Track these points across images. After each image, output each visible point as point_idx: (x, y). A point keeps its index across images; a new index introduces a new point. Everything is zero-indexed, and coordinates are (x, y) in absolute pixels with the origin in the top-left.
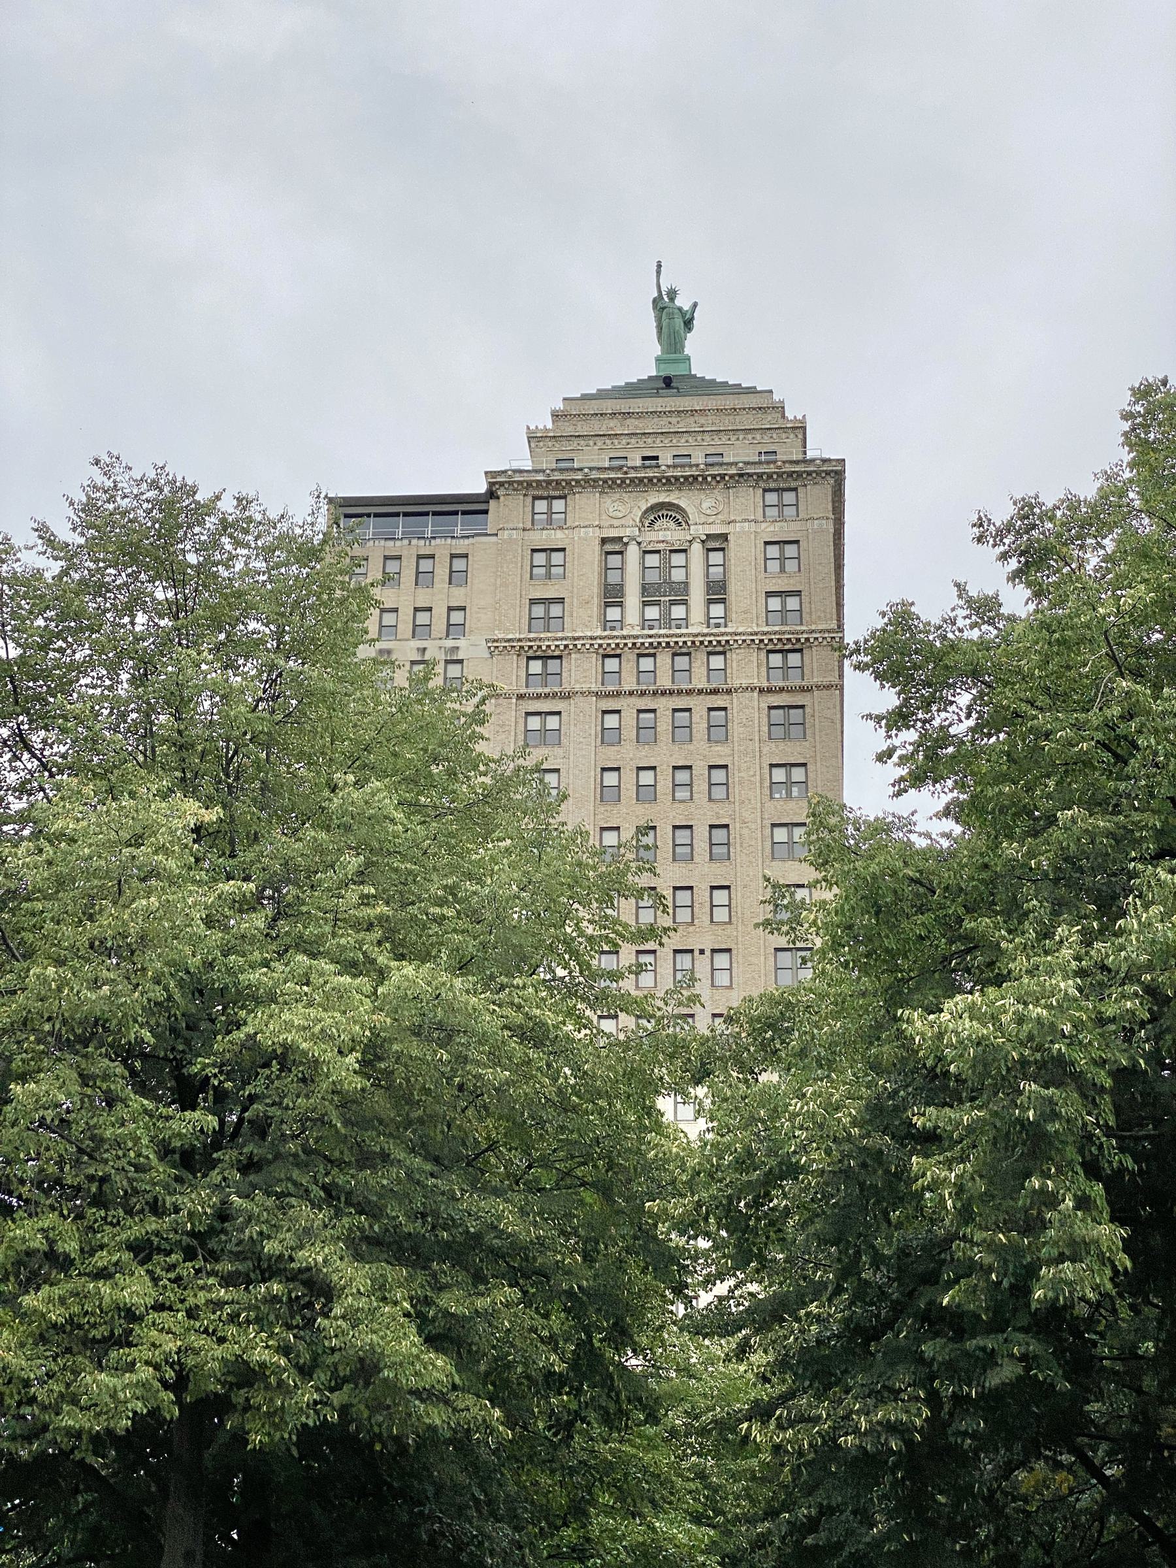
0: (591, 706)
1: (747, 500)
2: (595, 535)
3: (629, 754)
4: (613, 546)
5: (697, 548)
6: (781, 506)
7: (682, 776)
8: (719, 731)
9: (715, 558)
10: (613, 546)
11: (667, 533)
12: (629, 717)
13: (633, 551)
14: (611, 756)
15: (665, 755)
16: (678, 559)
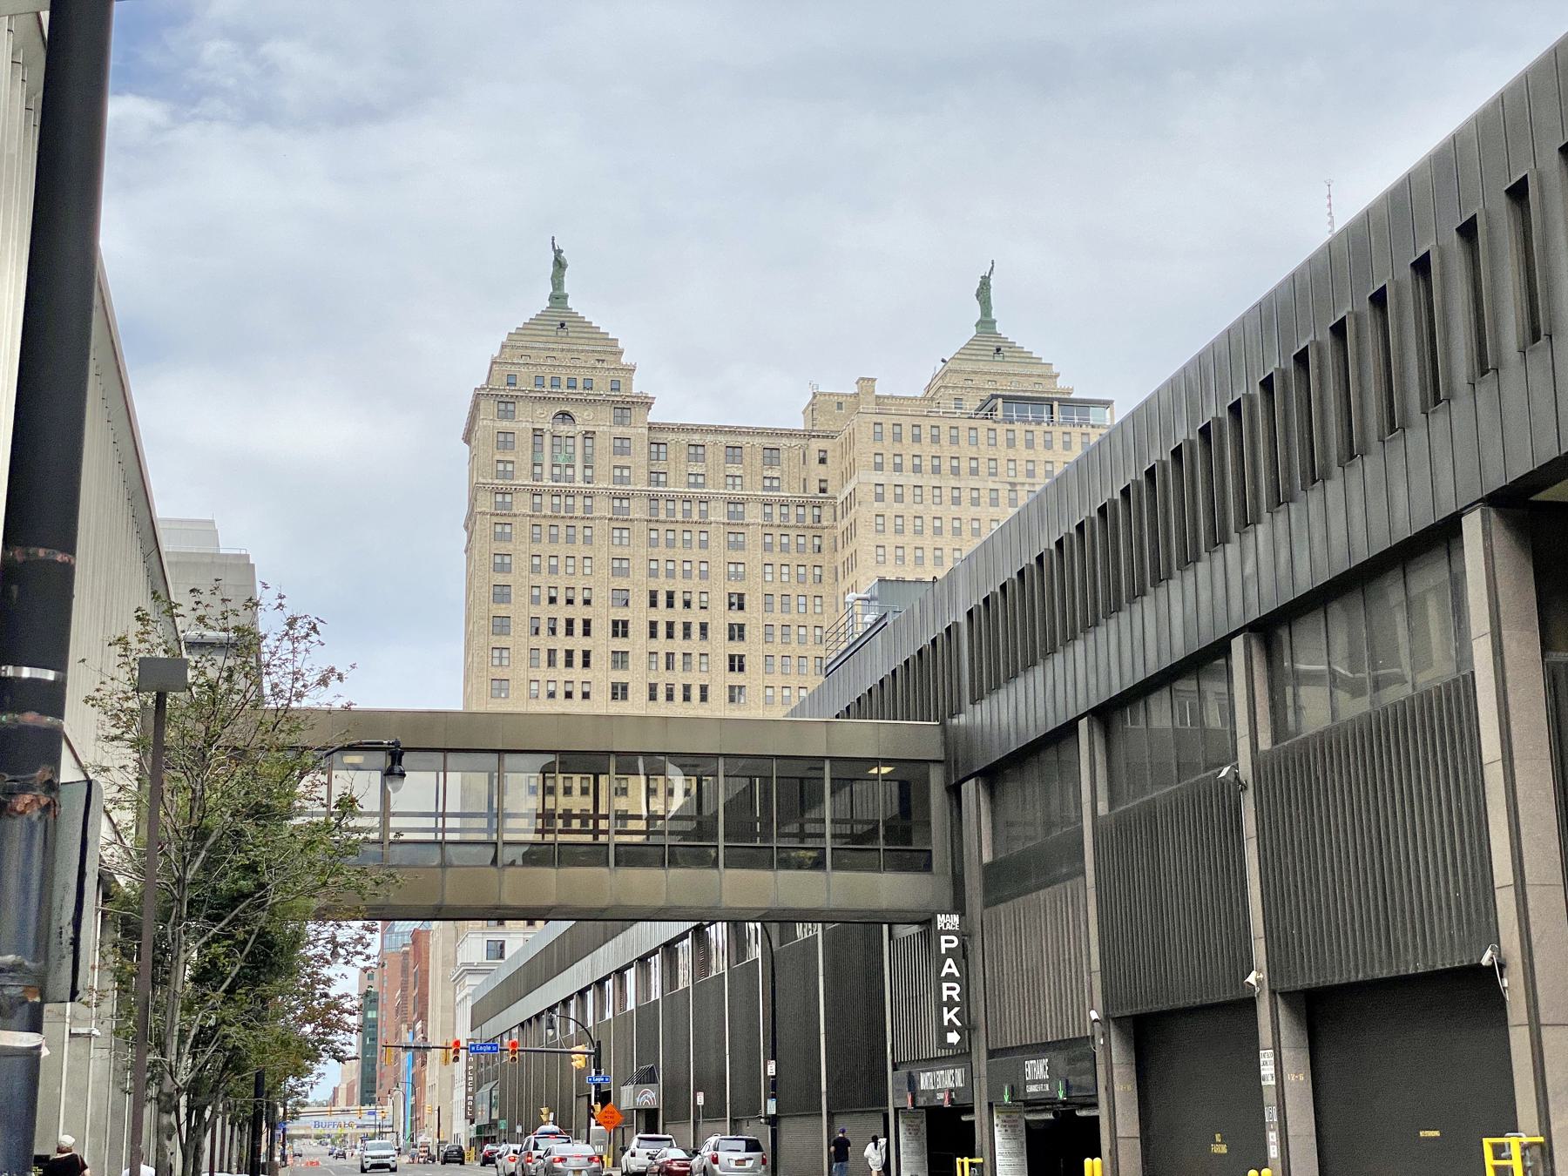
0: (527, 522)
1: (607, 414)
2: (530, 426)
3: (545, 548)
4: (537, 433)
5: (579, 439)
6: (622, 417)
7: (570, 562)
8: (588, 540)
9: (589, 442)
10: (537, 433)
11: (564, 429)
12: (545, 529)
13: (547, 437)
14: (535, 550)
15: (562, 549)
16: (570, 441)
